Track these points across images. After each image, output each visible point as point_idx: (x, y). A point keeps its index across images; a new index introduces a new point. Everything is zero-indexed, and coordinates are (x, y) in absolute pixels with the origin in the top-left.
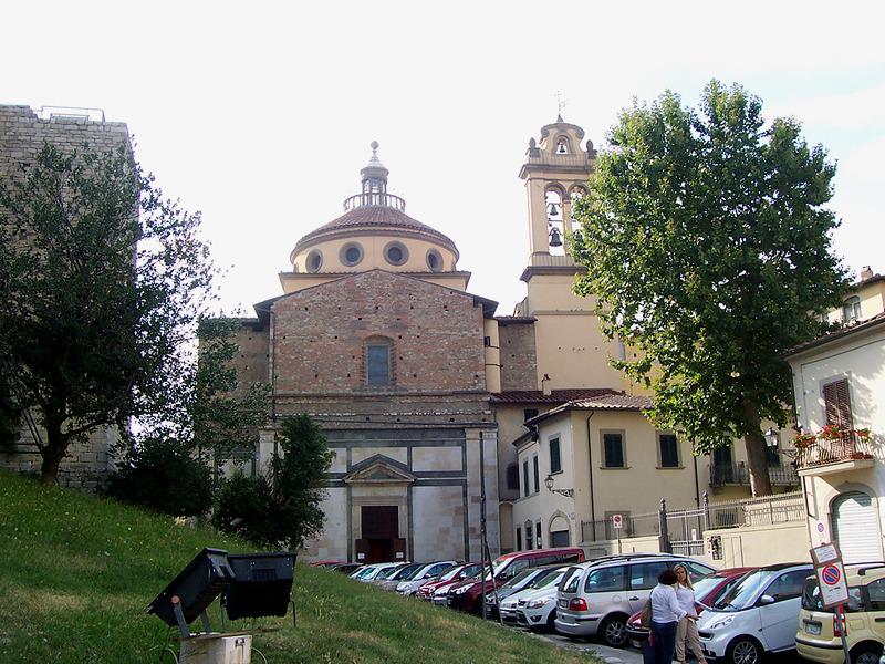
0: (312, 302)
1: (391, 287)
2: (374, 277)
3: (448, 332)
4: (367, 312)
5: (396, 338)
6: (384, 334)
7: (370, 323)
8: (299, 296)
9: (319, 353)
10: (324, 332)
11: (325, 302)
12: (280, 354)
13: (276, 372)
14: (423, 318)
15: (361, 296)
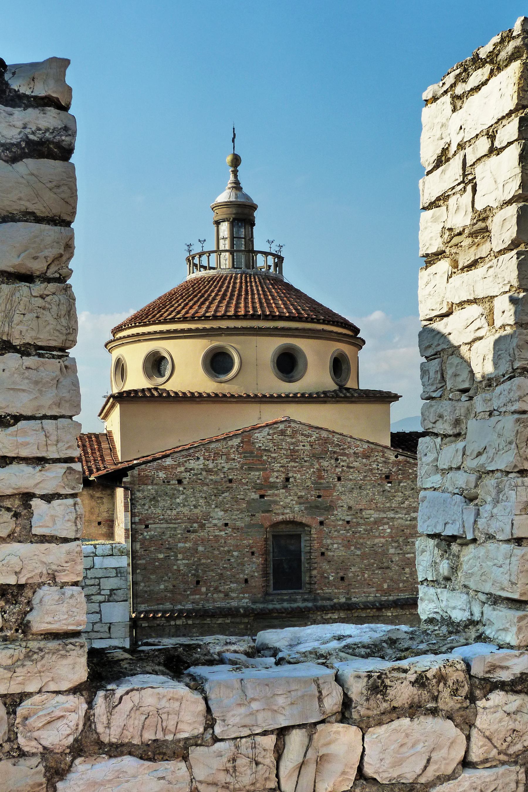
0: (186, 470)
1: (308, 447)
2: (283, 433)
3: (391, 515)
4: (273, 486)
5: (315, 525)
6: (298, 519)
7: (276, 503)
8: (169, 461)
9: (201, 548)
10: (207, 517)
11: (209, 471)
12: (141, 552)
13: (139, 578)
14: (355, 493)
15: (264, 463)
